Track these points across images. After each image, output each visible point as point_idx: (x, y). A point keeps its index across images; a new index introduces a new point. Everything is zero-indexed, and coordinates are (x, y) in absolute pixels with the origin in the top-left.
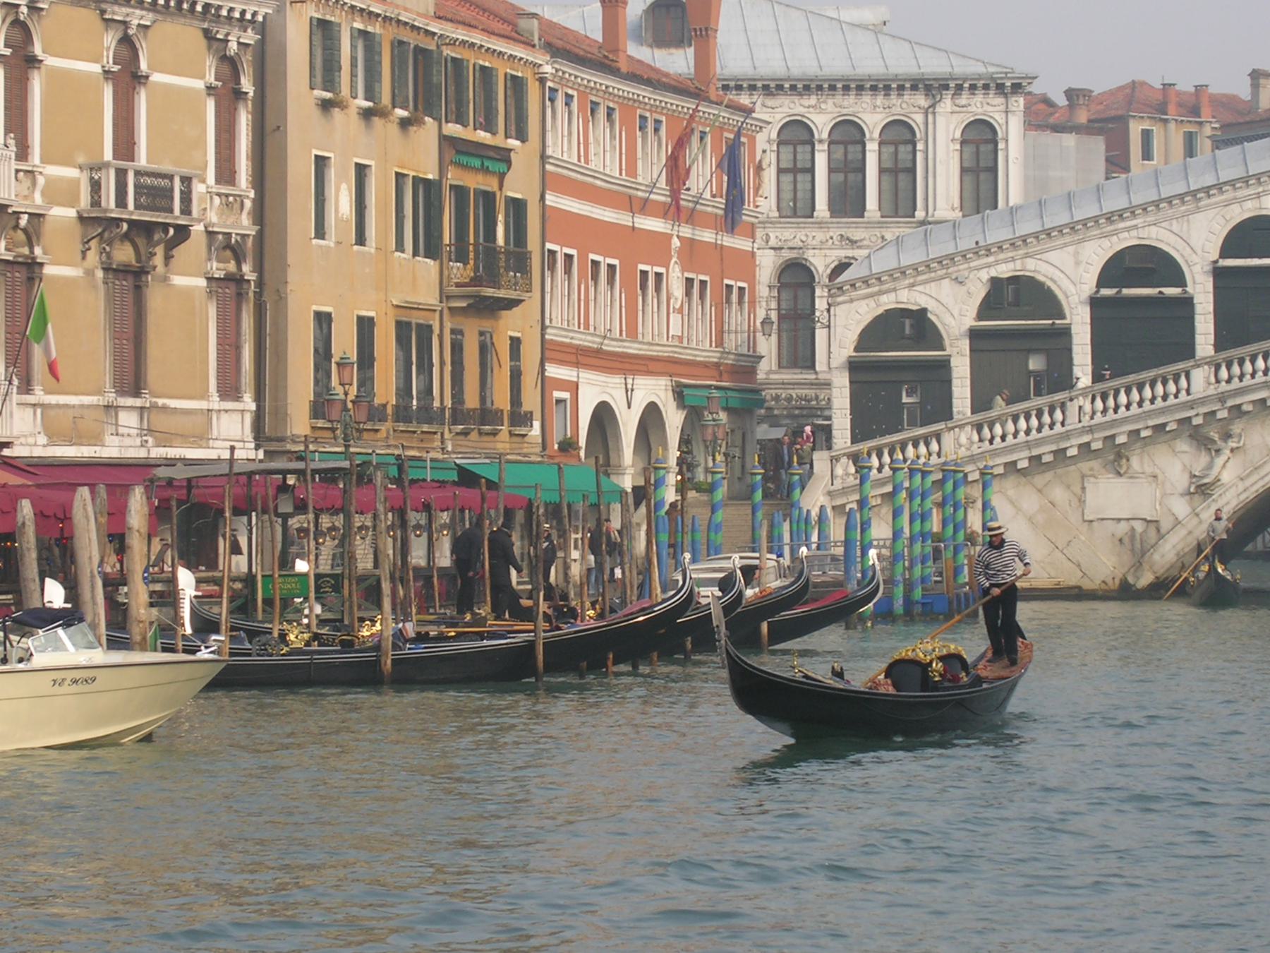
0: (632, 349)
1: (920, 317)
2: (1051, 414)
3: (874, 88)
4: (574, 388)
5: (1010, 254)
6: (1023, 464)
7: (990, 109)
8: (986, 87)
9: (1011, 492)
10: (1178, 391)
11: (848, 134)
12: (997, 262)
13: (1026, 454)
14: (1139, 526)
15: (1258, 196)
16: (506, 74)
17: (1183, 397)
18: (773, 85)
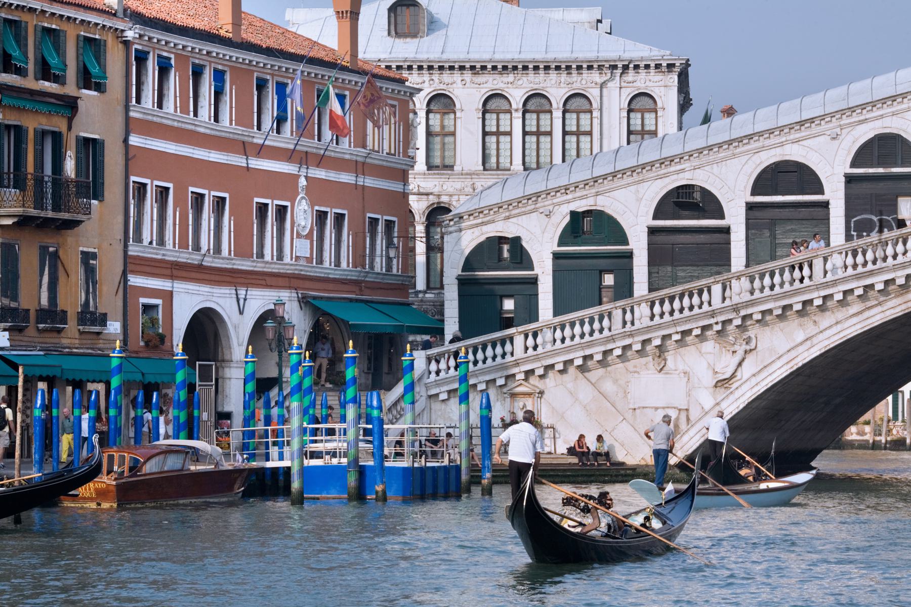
0: (245, 265)
1: (516, 242)
2: (601, 321)
3: (558, 68)
4: (168, 296)
5: (585, 193)
6: (579, 362)
7: (651, 84)
8: (647, 67)
9: (570, 386)
10: (702, 303)
11: (536, 102)
12: (575, 199)
13: (582, 353)
14: (673, 414)
15: (782, 144)
16: (78, 36)
17: (706, 307)
18: (478, 66)
